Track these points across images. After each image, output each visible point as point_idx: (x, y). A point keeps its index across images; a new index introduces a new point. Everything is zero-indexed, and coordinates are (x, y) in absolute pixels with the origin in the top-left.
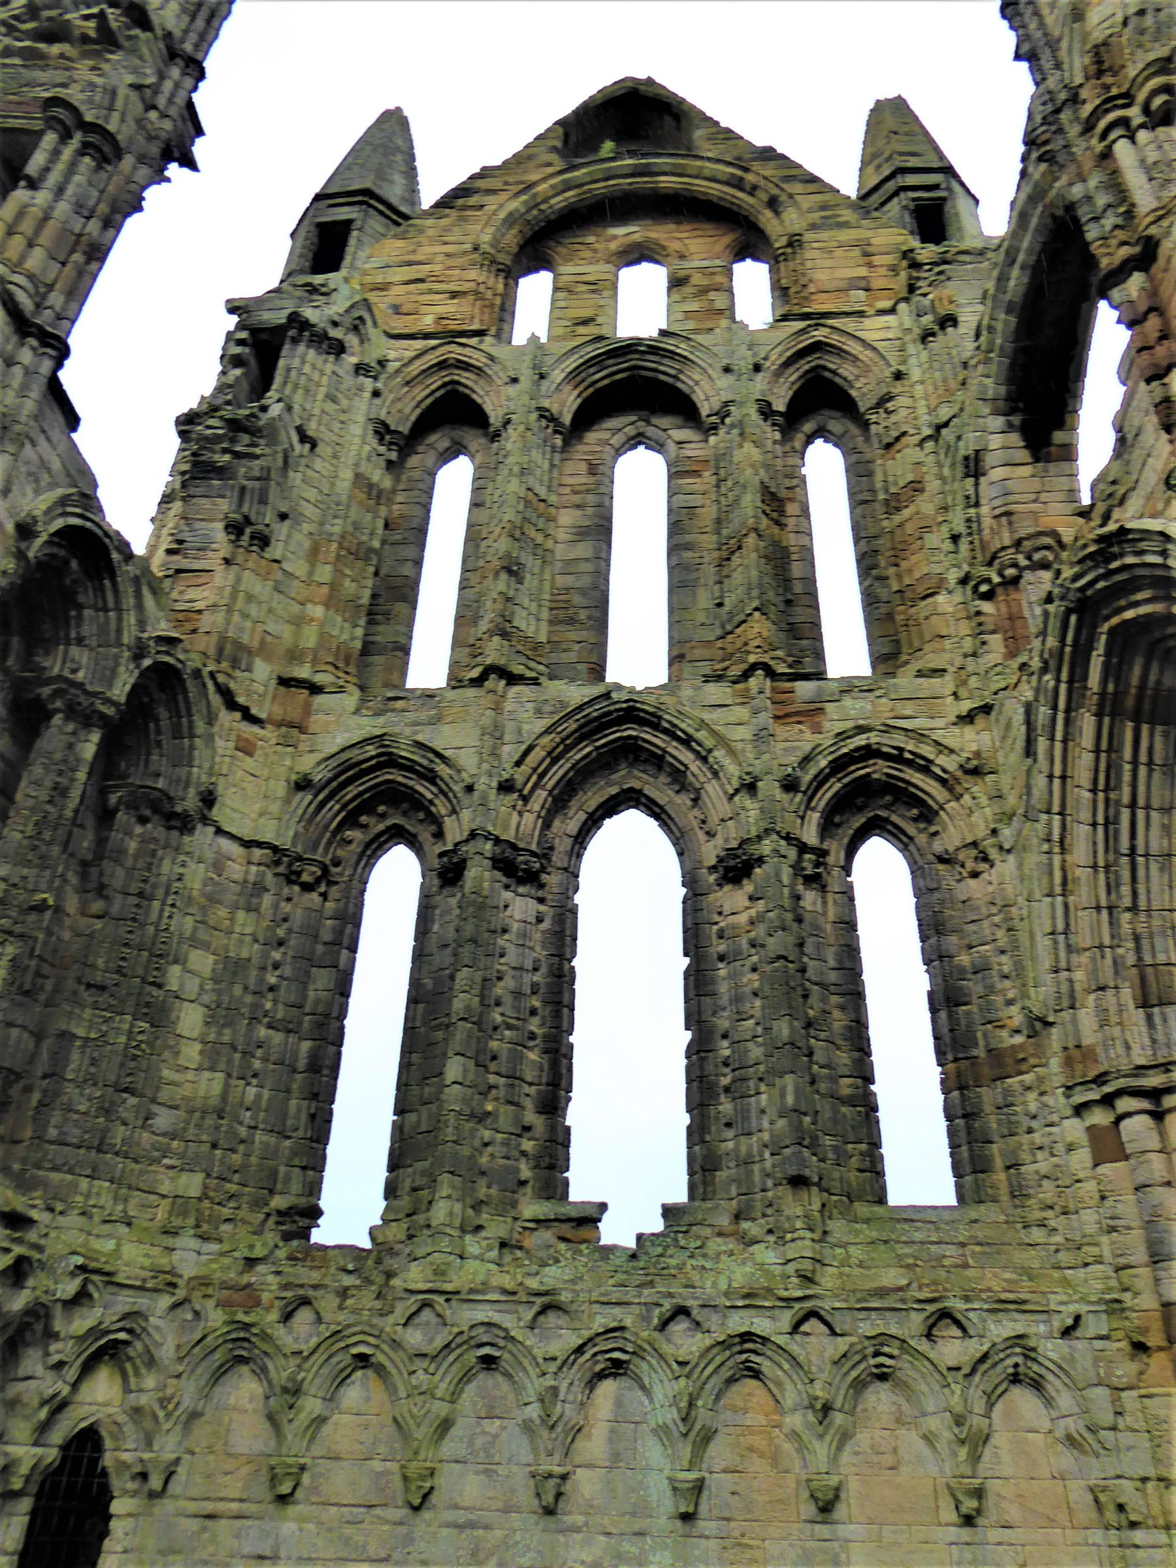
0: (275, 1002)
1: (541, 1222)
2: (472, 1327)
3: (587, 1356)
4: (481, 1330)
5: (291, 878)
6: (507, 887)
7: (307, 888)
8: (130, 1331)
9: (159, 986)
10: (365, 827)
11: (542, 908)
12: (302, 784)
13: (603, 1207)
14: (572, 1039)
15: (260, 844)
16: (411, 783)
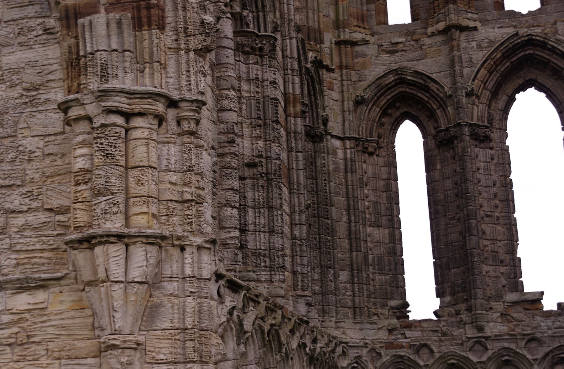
0: (370, 214)
1: (515, 303)
2: (499, 350)
3: (550, 357)
4: (502, 350)
5: (365, 151)
6: (476, 146)
7: (371, 154)
8: (357, 363)
9: (328, 219)
10: (391, 115)
11: (493, 152)
12: (359, 102)
13: (542, 293)
14: (515, 215)
15: (349, 138)
16: (415, 92)
